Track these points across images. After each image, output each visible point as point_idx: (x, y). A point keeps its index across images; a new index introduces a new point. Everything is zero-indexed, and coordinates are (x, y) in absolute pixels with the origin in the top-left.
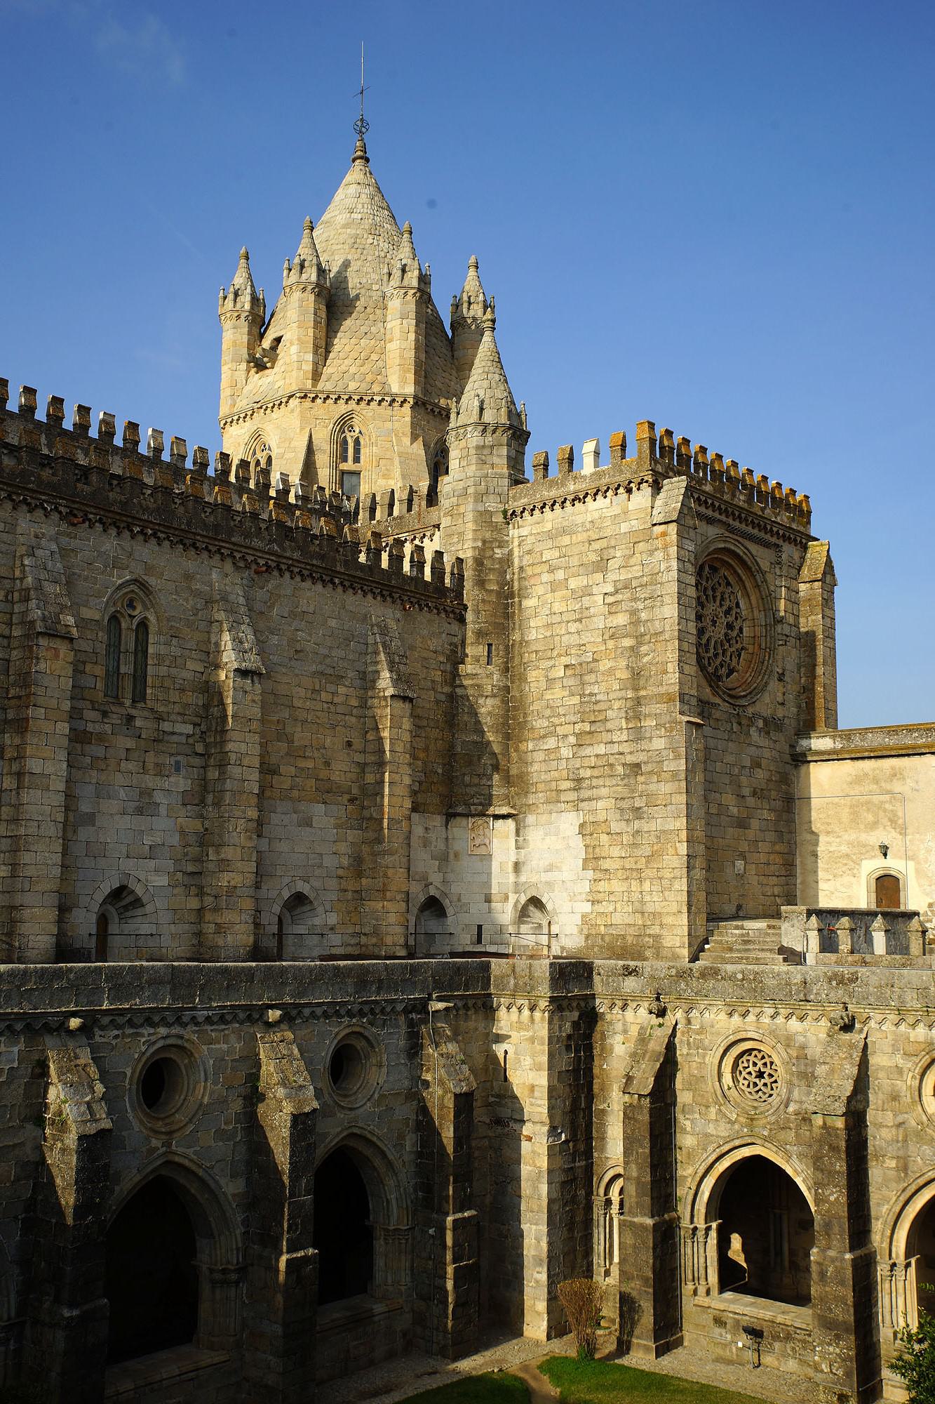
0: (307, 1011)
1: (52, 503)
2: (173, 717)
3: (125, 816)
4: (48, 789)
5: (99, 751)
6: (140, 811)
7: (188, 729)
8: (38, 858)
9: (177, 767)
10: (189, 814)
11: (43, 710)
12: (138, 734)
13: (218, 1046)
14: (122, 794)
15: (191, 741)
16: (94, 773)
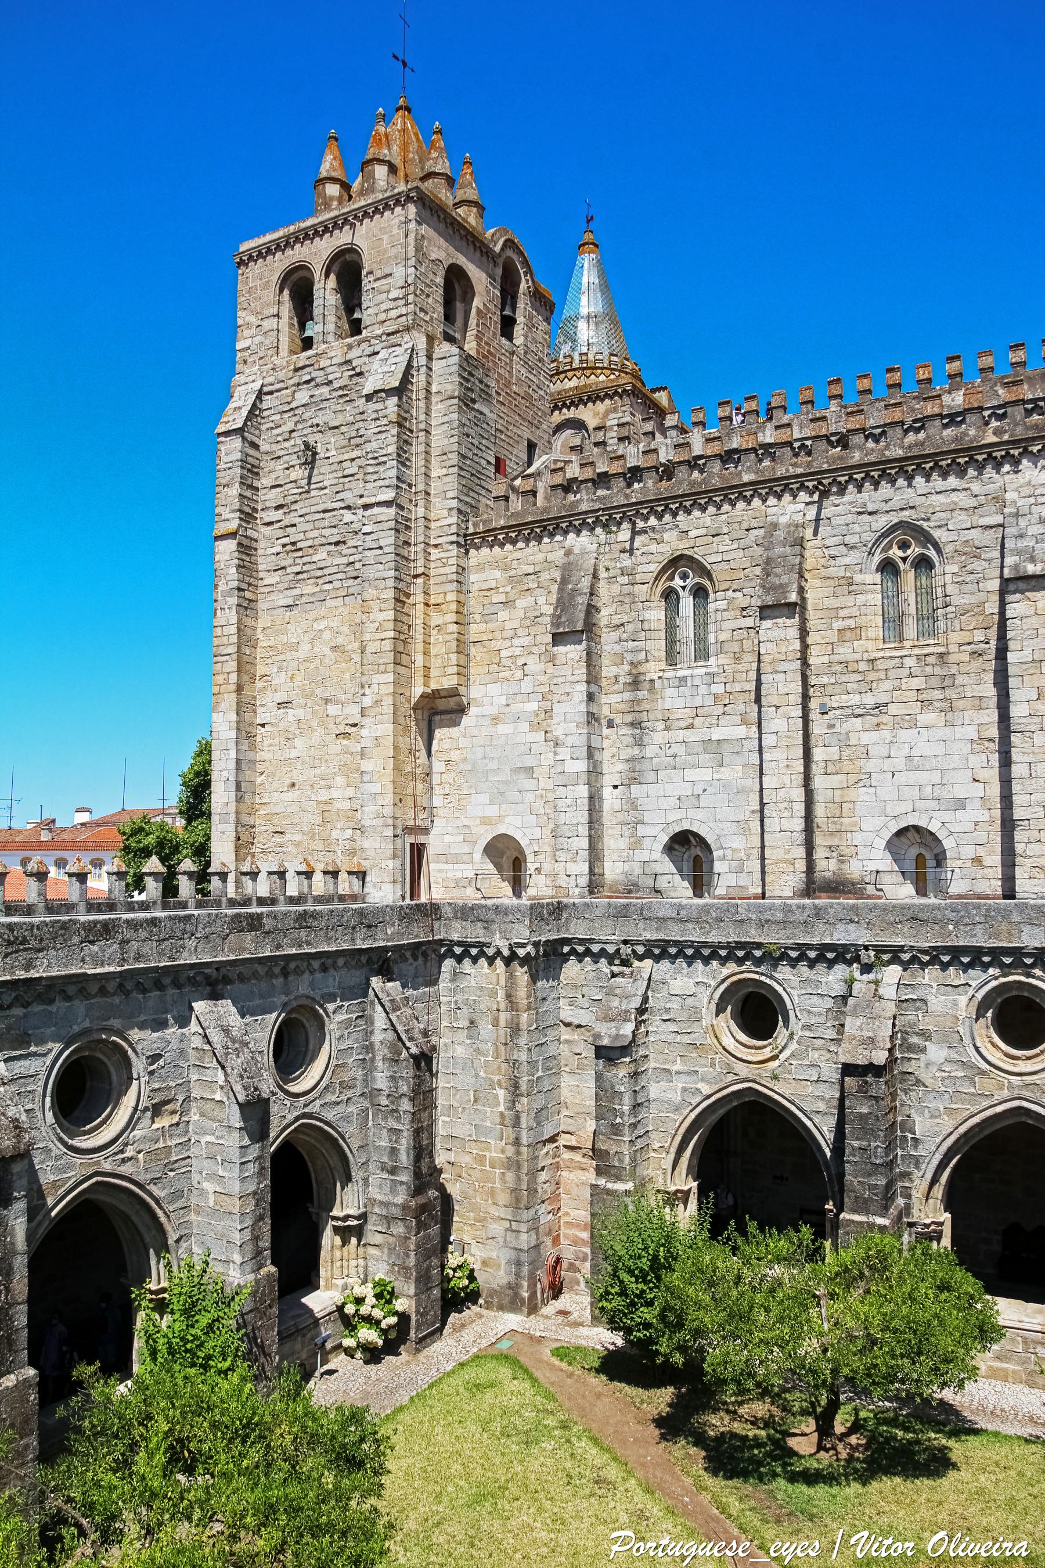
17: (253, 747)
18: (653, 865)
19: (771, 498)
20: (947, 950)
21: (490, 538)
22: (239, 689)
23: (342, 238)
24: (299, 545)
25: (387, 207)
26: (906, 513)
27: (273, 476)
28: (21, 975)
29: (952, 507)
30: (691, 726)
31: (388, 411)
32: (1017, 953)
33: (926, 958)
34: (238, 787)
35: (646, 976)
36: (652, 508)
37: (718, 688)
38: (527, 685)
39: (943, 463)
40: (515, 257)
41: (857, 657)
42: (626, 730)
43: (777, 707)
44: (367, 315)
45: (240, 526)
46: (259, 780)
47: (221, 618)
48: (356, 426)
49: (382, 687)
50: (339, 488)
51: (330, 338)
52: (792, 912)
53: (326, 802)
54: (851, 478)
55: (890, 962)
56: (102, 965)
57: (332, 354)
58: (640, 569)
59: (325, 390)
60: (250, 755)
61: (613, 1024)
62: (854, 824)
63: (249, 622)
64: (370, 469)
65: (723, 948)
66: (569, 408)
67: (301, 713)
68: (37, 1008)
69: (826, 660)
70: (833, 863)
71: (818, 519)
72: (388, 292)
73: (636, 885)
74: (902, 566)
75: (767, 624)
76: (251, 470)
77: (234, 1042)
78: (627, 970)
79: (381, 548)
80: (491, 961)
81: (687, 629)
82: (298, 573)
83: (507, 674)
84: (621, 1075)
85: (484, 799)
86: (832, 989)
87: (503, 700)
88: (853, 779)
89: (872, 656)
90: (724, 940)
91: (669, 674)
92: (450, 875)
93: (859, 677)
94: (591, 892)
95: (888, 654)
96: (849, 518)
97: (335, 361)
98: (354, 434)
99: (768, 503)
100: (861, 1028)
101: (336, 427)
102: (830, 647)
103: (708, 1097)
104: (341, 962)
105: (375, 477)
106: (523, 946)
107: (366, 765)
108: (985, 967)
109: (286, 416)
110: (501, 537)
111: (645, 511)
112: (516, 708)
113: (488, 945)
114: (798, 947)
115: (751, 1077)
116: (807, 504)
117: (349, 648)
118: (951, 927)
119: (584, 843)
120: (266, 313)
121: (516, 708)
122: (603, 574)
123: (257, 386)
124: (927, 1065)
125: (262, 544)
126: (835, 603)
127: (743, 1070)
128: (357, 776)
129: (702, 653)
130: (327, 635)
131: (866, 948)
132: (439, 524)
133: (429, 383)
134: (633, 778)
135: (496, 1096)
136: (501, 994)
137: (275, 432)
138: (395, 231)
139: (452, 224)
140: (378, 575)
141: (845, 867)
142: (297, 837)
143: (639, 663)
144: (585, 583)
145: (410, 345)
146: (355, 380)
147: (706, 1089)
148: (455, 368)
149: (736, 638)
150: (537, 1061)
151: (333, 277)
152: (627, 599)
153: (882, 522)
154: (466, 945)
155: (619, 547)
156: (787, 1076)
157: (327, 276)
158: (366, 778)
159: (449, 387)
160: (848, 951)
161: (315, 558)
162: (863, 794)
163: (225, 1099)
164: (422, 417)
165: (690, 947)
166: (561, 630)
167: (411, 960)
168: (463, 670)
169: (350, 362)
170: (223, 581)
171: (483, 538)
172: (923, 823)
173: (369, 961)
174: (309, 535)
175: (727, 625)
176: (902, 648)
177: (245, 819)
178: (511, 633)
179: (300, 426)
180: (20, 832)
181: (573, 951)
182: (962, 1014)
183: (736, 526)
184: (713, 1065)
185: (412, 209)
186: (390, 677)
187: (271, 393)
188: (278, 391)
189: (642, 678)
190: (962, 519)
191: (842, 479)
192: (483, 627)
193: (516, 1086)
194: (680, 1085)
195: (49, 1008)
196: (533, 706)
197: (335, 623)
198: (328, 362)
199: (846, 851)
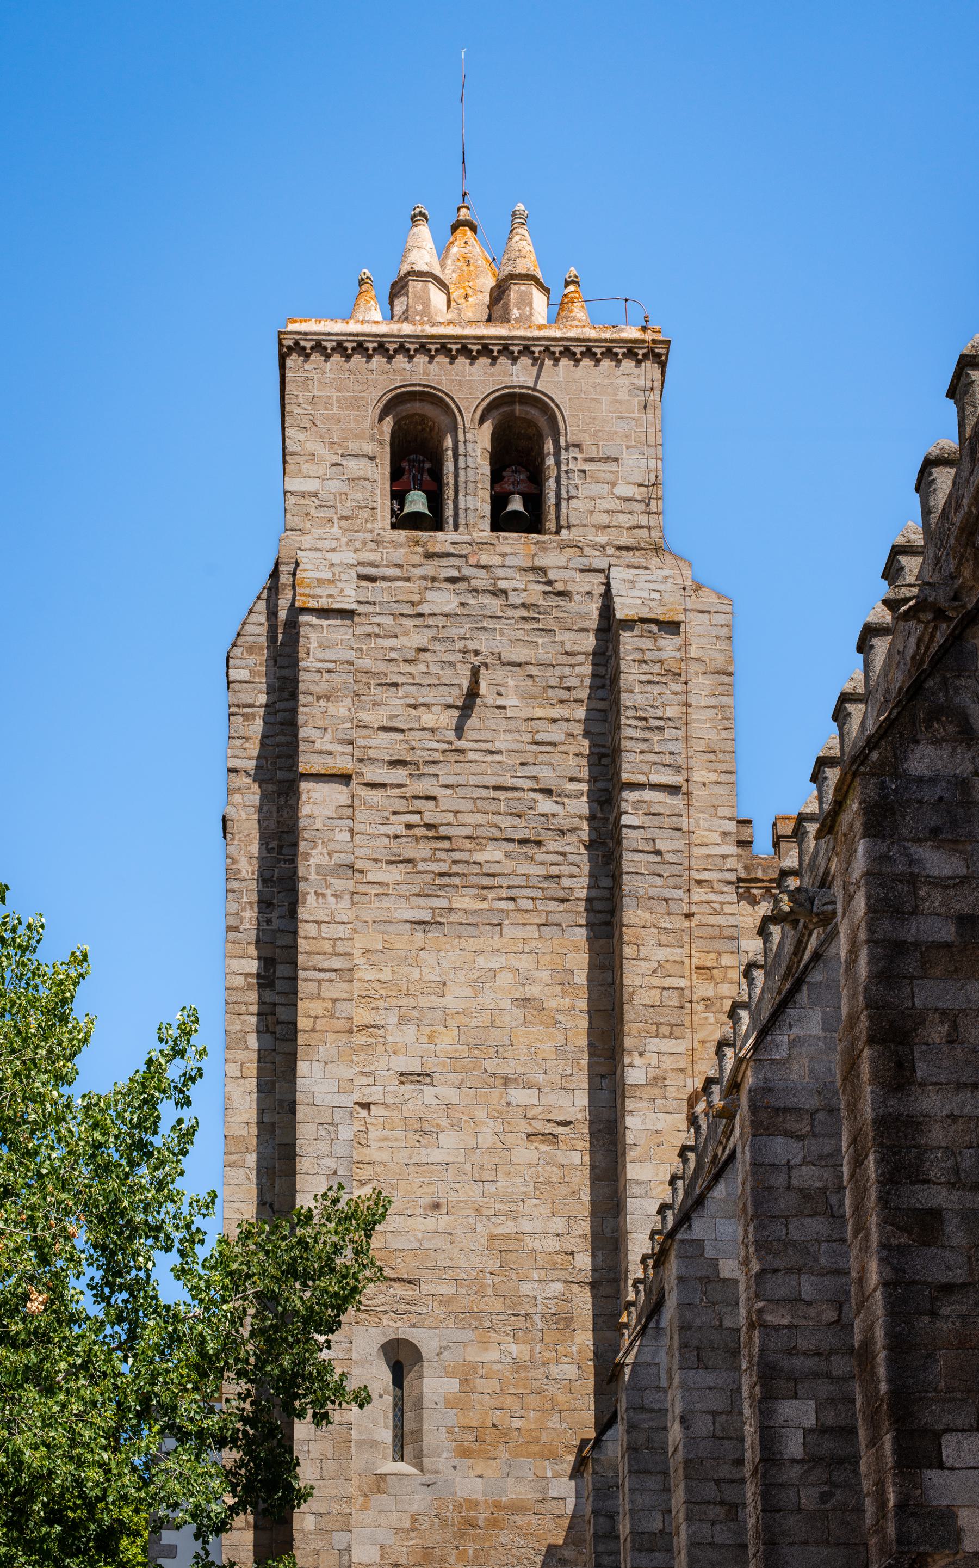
24: (443, 831)
48: (558, 671)
49: (664, 1058)
50: (529, 758)
53: (507, 1237)
59: (494, 604)
67: (452, 1095)
72: (614, 484)
82: (441, 875)
97: (510, 561)
98: (554, 682)
101: (520, 665)
109: (409, 623)
117: (552, 1004)
120: (354, 447)
130: (505, 978)
138: (623, 395)
142: (446, 1290)
161: (478, 857)
169: (543, 570)
187: (372, 579)
188: (384, 579)
197: (524, 962)
198: (497, 560)
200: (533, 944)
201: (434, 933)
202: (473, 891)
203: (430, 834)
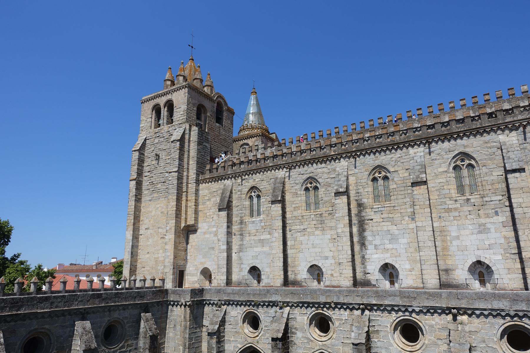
0: (478, 312)
1: (419, 141)
2: (489, 195)
3: (474, 235)
4: (425, 231)
5: (457, 214)
6: (480, 232)
7: (500, 198)
8: (426, 254)
9: (497, 213)
10: (507, 230)
11: (418, 206)
12: (473, 204)
13: (429, 321)
14: (470, 227)
15: (502, 202)
16: (455, 222)
17: (138, 241)
18: (245, 276)
19: (277, 170)
20: (301, 302)
21: (205, 181)
22: (134, 224)
23: (169, 97)
24: (154, 183)
25: (180, 89)
26: (311, 174)
27: (148, 163)
28: (15, 313)
29: (323, 172)
30: (256, 235)
31: (177, 146)
32: (319, 303)
33: (296, 305)
34: (132, 253)
35: (224, 310)
36: (246, 173)
37: (263, 224)
38: (213, 223)
39: (320, 160)
40: (222, 100)
41: (299, 215)
42: (239, 236)
43: (276, 230)
44: (174, 118)
45: (137, 177)
46: (139, 251)
47: (130, 203)
49: (172, 224)
51: (165, 124)
52: (261, 291)
53: (157, 258)
54: (297, 165)
55: (286, 307)
56: (44, 309)
57: (165, 129)
58: (243, 190)
59: (162, 139)
60: (136, 244)
61: (213, 326)
62: (299, 264)
63: (139, 204)
64: (172, 162)
65: (244, 302)
66: (245, 140)
68: (19, 322)
69: (290, 216)
70: (293, 275)
71: (289, 176)
72: (180, 112)
73: (240, 283)
74: (310, 189)
75: (273, 206)
76: (141, 161)
77: (86, 331)
78: (219, 309)
79: (173, 184)
80: (181, 306)
81: (255, 208)
82: (153, 191)
83: (209, 220)
84: (214, 341)
85: (201, 257)
86: (272, 314)
87: (207, 227)
88: (298, 250)
89: (303, 214)
90: (244, 299)
91: (250, 220)
92: (191, 280)
93: (299, 221)
94: (227, 285)
95: (307, 214)
96: (297, 176)
97: (166, 131)
99: (276, 172)
100: (276, 327)
101: (165, 150)
102: (291, 212)
103: (241, 349)
104: (130, 307)
105: (173, 164)
106: (189, 301)
107: (167, 247)
108: (312, 308)
109: (152, 146)
110: (208, 181)
111: (244, 174)
112: (210, 230)
113: (180, 302)
114: (263, 302)
115: (251, 342)
116: (286, 172)
118: (301, 296)
119: (225, 270)
121: (210, 230)
122: (234, 192)
123: (144, 137)
124: (297, 338)
125: (144, 182)
126: (293, 199)
127: (250, 340)
128: (165, 250)
129: (259, 214)
130: (160, 209)
131: (280, 302)
132: (191, 177)
133: (189, 138)
134: (240, 250)
135: (180, 349)
136: (183, 317)
137: (149, 150)
138: (182, 96)
139: (200, 93)
140: (172, 192)
141: (296, 277)
142: (149, 269)
143: (243, 217)
144: (228, 194)
145: (184, 127)
146: (170, 136)
147: (240, 346)
148: (197, 134)
149: (267, 210)
150: (193, 338)
151: (166, 108)
152: (240, 198)
153: (305, 177)
154: (174, 302)
155: (238, 184)
156: (261, 342)
157: (165, 107)
158: (166, 251)
159: (195, 139)
160: (275, 303)
161: (158, 187)
162: (301, 255)
163: (80, 349)
164: (187, 147)
165: (236, 302)
166: (220, 208)
167: (157, 306)
168: (196, 219)
169: (169, 131)
170: (131, 193)
171: (203, 181)
172: (317, 264)
173: (141, 307)
174: (156, 180)
175: (265, 206)
176: (311, 212)
177: (134, 264)
178: (210, 208)
179: (156, 149)
180: (87, 266)
181: (206, 303)
182: (306, 323)
183: (268, 178)
184: (241, 338)
185: (187, 89)
186: (174, 221)
187: (148, 139)
189: (243, 221)
190: (326, 176)
191: (295, 165)
192: (202, 206)
193: (185, 346)
194: (233, 345)
195: (24, 322)
196: (215, 229)
197: (162, 205)
198: (163, 131)
199: (296, 272)
200: (164, 201)
201: (152, 201)
202: (157, 193)
203: (152, 183)
